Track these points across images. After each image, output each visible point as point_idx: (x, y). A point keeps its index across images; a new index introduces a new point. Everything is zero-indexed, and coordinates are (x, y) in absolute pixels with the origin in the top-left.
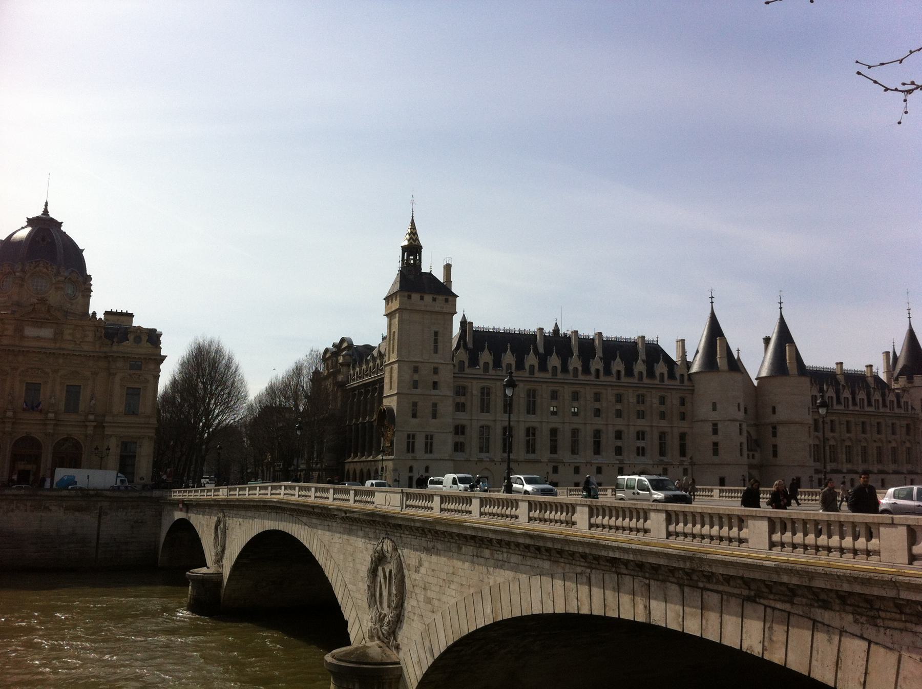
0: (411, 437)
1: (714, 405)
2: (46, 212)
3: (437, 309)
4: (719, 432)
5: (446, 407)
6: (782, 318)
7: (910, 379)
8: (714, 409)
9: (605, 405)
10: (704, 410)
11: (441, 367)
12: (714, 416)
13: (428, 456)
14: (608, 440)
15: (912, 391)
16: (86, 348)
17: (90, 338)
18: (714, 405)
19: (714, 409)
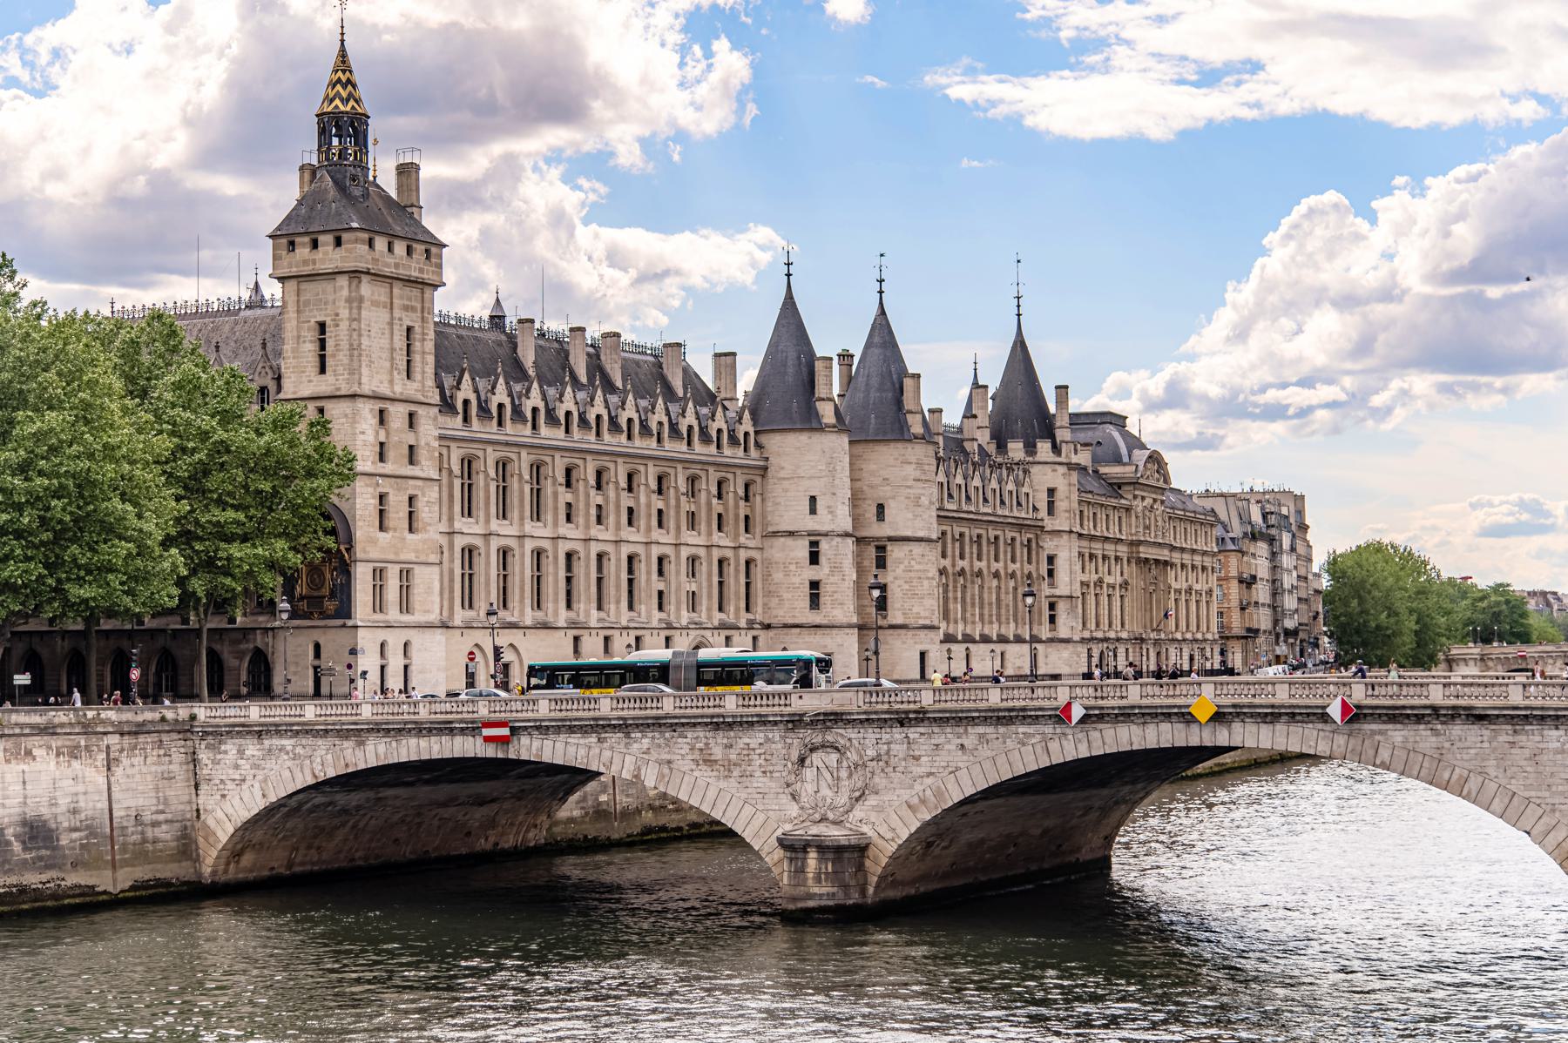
0: (379, 574)
1: (813, 499)
3: (415, 274)
4: (822, 559)
6: (882, 312)
7: (1030, 448)
8: (813, 511)
9: (643, 499)
11: (421, 411)
12: (811, 524)
13: (406, 618)
14: (648, 581)
15: (1034, 470)
18: (813, 499)
19: (813, 511)
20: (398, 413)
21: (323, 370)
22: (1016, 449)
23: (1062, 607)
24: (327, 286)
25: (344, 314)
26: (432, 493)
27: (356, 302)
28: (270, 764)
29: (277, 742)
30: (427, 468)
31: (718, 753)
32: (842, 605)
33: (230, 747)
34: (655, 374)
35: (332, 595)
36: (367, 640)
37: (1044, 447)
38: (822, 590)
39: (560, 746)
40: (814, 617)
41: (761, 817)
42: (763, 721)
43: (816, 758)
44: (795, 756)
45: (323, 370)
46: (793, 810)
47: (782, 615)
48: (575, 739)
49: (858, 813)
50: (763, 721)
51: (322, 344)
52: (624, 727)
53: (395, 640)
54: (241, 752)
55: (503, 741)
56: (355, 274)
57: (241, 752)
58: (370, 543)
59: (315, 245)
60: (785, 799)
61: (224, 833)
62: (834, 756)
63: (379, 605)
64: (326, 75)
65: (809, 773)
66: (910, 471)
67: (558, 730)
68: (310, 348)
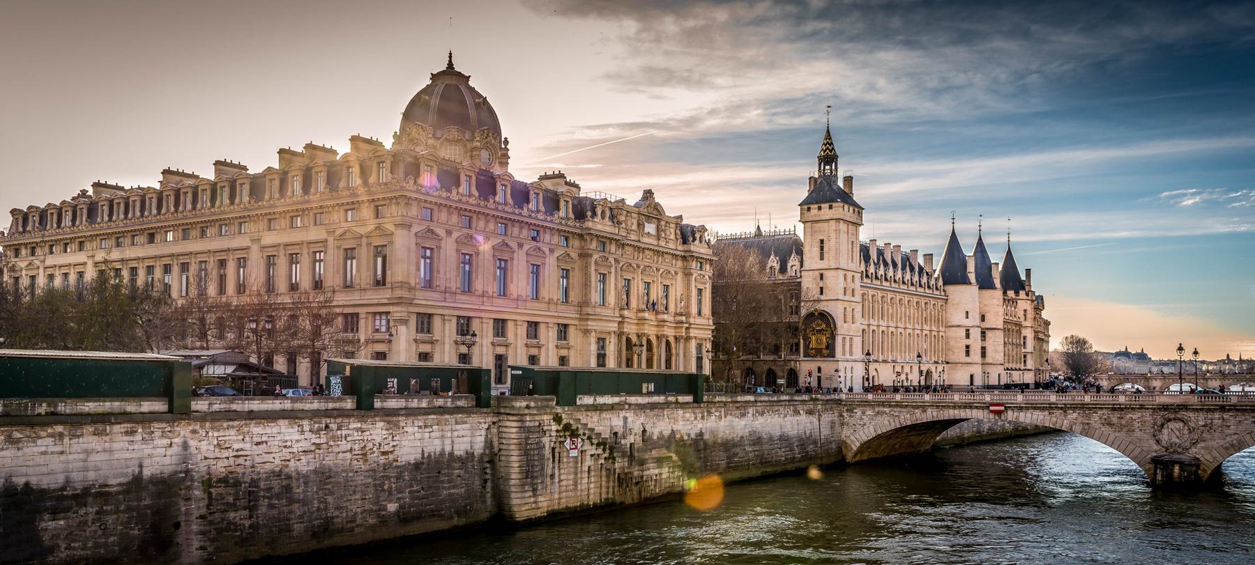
2: (450, 65)
5: (858, 315)
7: (1017, 293)
10: (957, 318)
16: (671, 245)
17: (672, 237)
20: (850, 275)
21: (822, 259)
22: (1011, 294)
23: (1029, 357)
24: (825, 225)
25: (833, 235)
26: (859, 308)
27: (838, 231)
28: (879, 418)
29: (881, 409)
30: (858, 298)
31: (1115, 420)
32: (976, 356)
33: (858, 412)
34: (907, 262)
35: (827, 348)
36: (841, 366)
37: (1022, 293)
38: (971, 349)
39: (1029, 415)
40: (968, 360)
41: (1139, 450)
42: (1142, 407)
43: (1172, 425)
44: (1159, 423)
45: (822, 259)
46: (1155, 447)
47: (952, 358)
48: (1037, 413)
49: (1194, 450)
50: (1142, 407)
51: (822, 249)
52: (1065, 409)
53: (848, 365)
54: (863, 413)
55: (999, 413)
56: (838, 220)
57: (863, 413)
58: (842, 328)
59: (820, 208)
60: (1152, 442)
61: (855, 446)
62: (1181, 424)
63: (844, 354)
64: (822, 141)
65: (1165, 431)
66: (995, 301)
67: (1027, 408)
68: (817, 250)
